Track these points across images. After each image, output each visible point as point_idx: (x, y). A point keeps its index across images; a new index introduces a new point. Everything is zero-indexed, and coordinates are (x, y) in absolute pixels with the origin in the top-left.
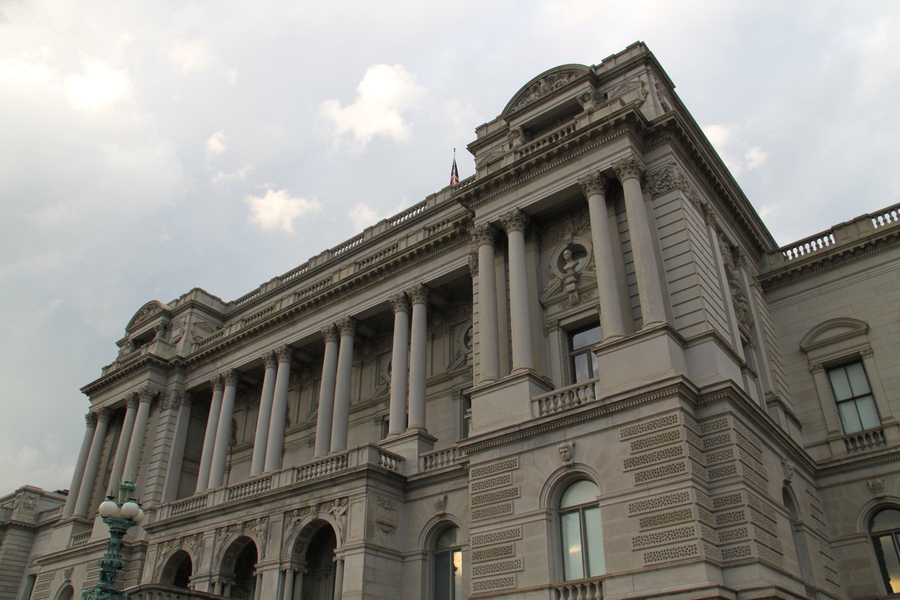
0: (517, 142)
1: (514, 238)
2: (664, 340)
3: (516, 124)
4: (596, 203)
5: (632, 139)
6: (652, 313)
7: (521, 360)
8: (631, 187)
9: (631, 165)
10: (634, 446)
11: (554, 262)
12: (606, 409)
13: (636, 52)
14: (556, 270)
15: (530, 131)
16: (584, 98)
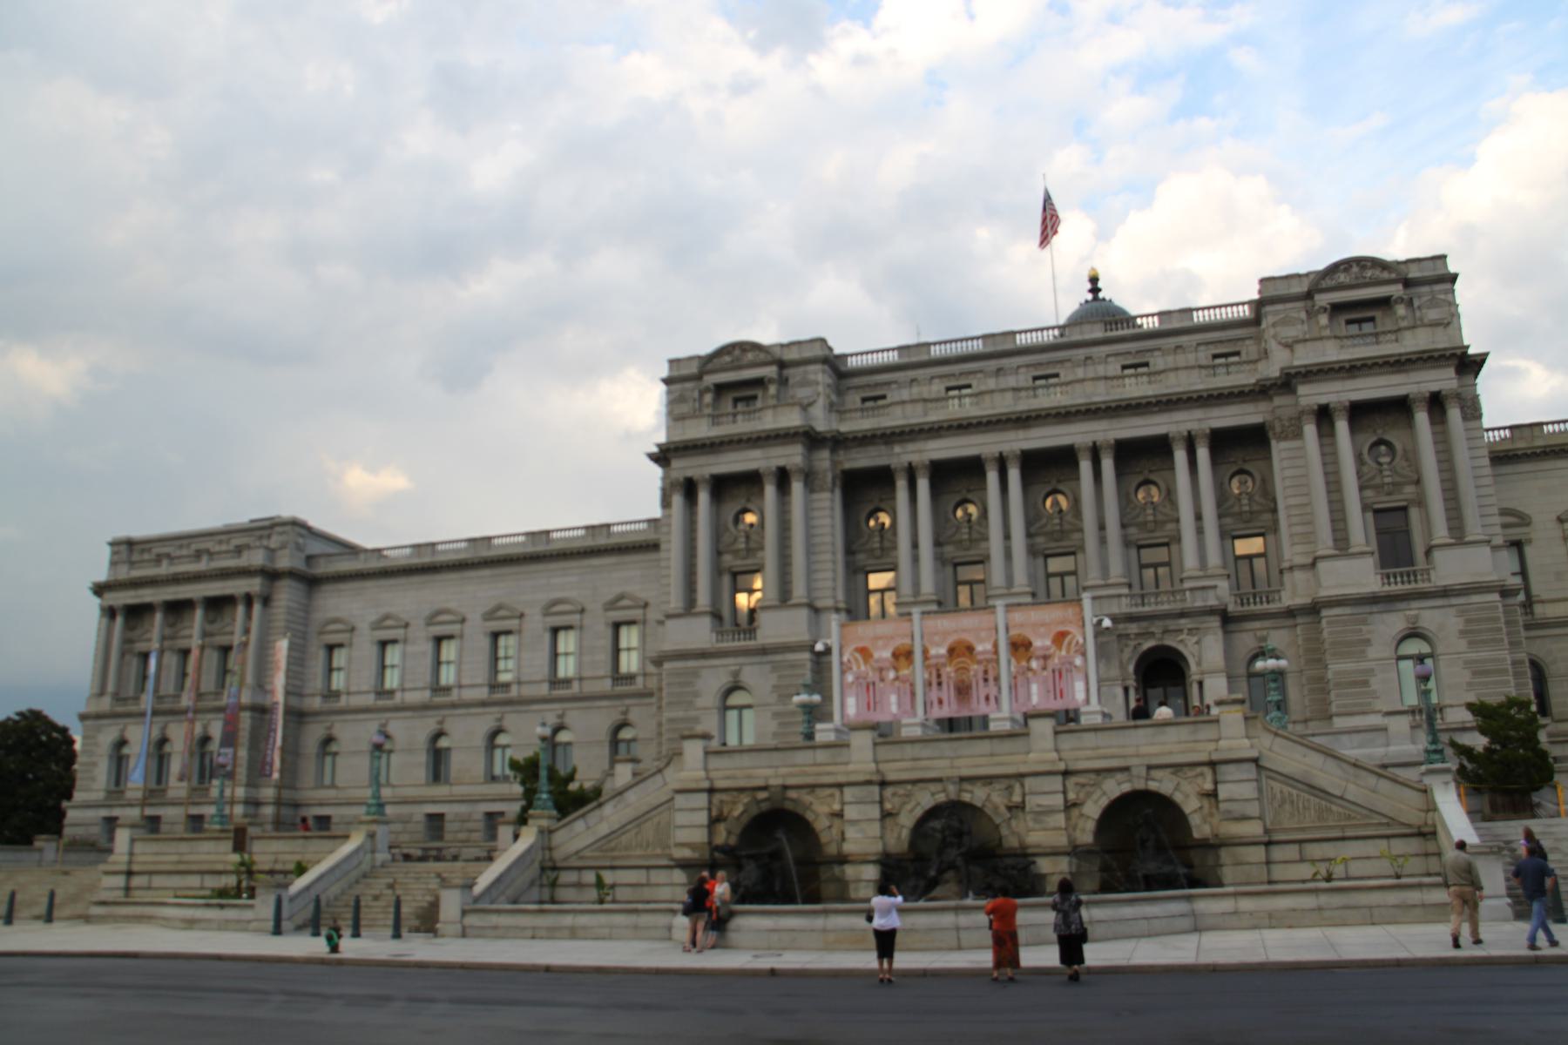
0: (708, 398)
1: (703, 497)
2: (803, 614)
3: (710, 380)
4: (770, 491)
5: (804, 444)
6: (799, 591)
7: (703, 599)
8: (797, 487)
9: (801, 471)
10: (780, 677)
11: (730, 518)
12: (764, 651)
13: (818, 352)
14: (731, 526)
15: (720, 389)
16: (771, 381)
